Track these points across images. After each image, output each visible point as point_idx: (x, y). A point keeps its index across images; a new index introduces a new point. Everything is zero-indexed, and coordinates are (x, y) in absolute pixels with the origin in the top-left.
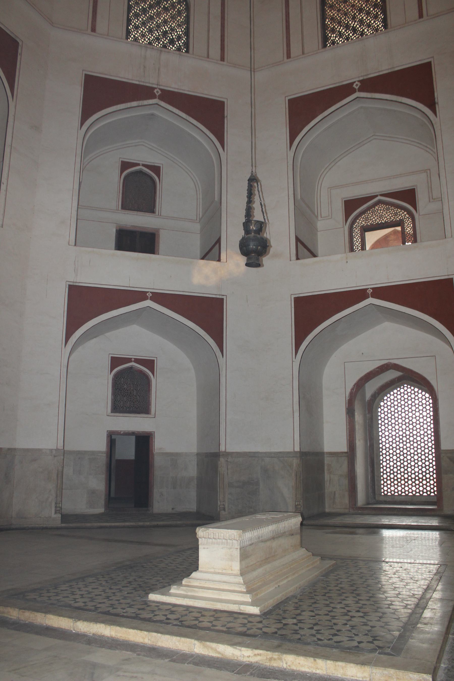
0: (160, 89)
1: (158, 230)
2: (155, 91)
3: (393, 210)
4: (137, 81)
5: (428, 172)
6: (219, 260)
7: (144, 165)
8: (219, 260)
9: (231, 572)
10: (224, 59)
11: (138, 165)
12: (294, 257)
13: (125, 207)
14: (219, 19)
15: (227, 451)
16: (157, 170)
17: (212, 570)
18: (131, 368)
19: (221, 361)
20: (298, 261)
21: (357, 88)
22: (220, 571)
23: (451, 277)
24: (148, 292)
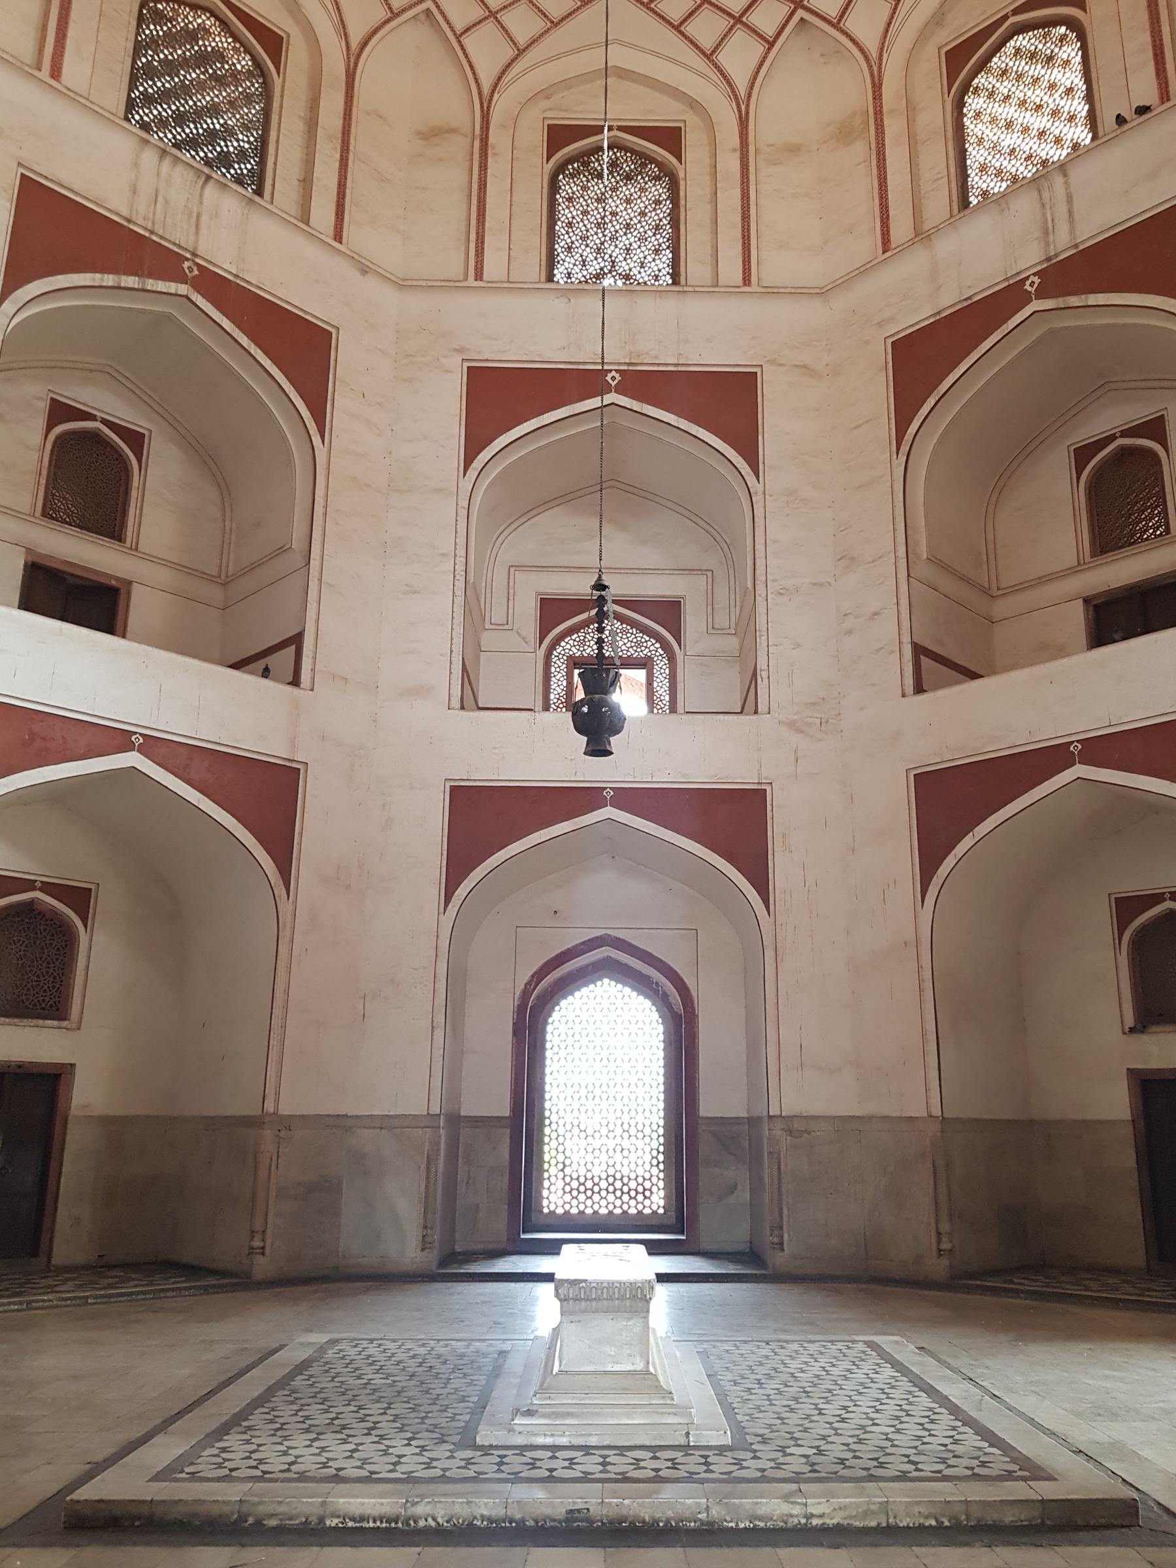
0: (198, 265)
1: (130, 583)
2: (186, 265)
3: (636, 636)
4: (146, 229)
5: (710, 574)
6: (295, 682)
7: (105, 422)
8: (295, 682)
10: (341, 238)
11: (93, 418)
12: (456, 703)
13: (50, 512)
14: (338, 143)
15: (284, 1110)
16: (136, 440)
18: (32, 902)
19: (285, 907)
20: (462, 713)
21: (613, 384)
24: (135, 733)
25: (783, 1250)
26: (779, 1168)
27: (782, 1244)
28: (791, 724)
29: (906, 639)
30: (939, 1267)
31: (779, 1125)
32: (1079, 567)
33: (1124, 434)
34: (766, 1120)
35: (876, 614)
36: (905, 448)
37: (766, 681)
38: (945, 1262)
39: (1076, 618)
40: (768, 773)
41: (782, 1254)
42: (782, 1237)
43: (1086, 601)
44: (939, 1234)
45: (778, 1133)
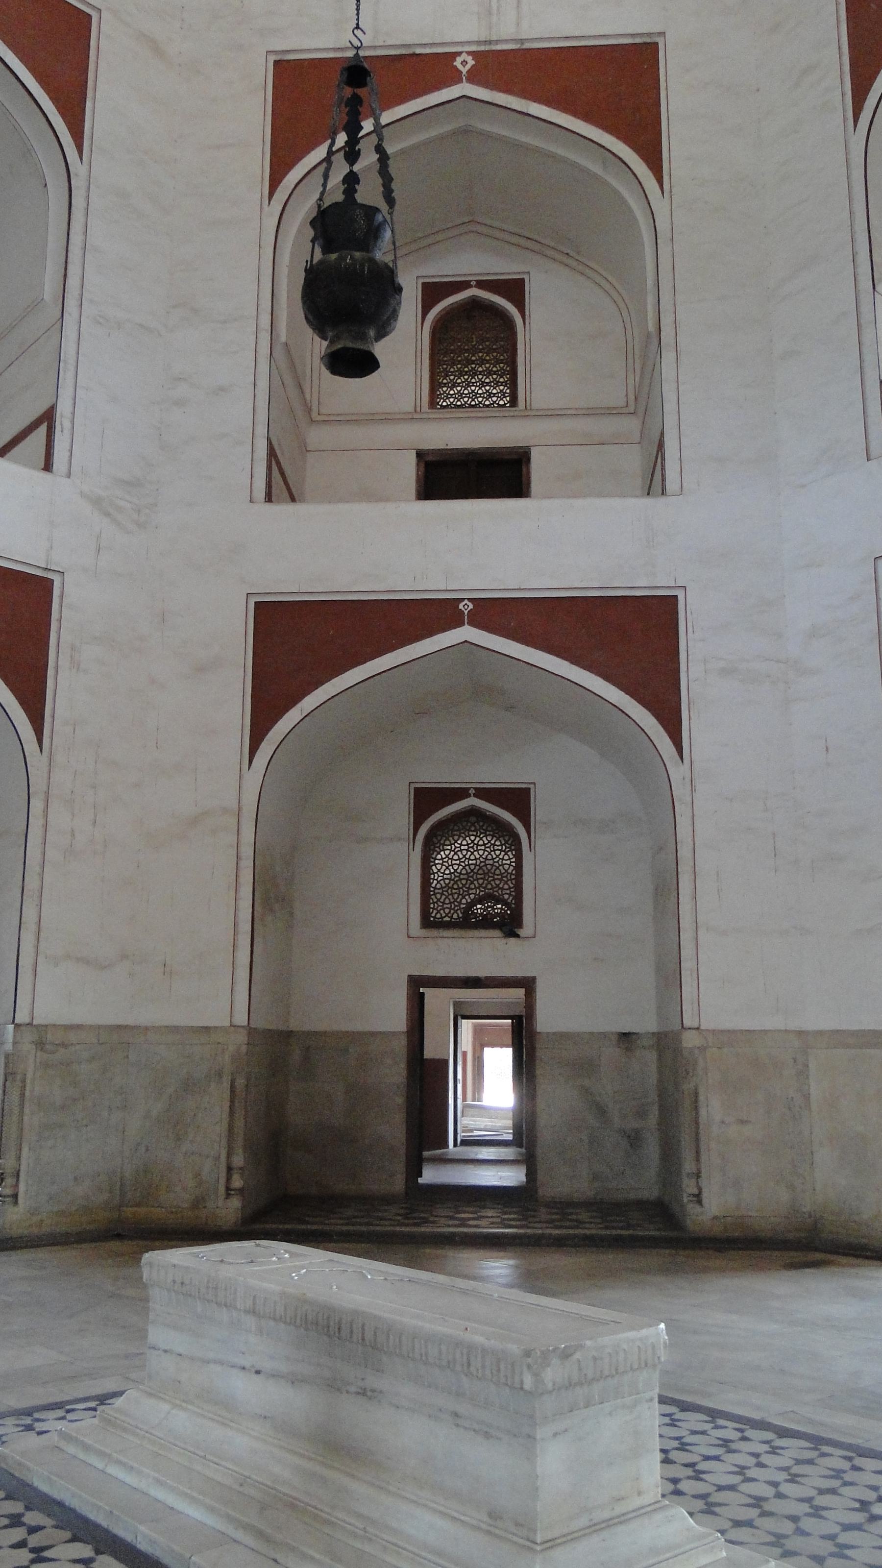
9: (638, 1502)
17: (583, 1521)
22: (606, 1514)
23: (50, 575)
25: (16, 1203)
26: (23, 1095)
27: (15, 1196)
28: (97, 502)
29: (262, 430)
30: (229, 1210)
31: (28, 1037)
32: (412, 417)
33: (481, 284)
34: (11, 1027)
35: (222, 389)
36: (281, 194)
37: (67, 432)
38: (236, 1203)
39: (408, 471)
40: (59, 560)
41: (16, 1209)
42: (17, 1185)
43: (420, 454)
44: (230, 1169)
45: (27, 1047)
